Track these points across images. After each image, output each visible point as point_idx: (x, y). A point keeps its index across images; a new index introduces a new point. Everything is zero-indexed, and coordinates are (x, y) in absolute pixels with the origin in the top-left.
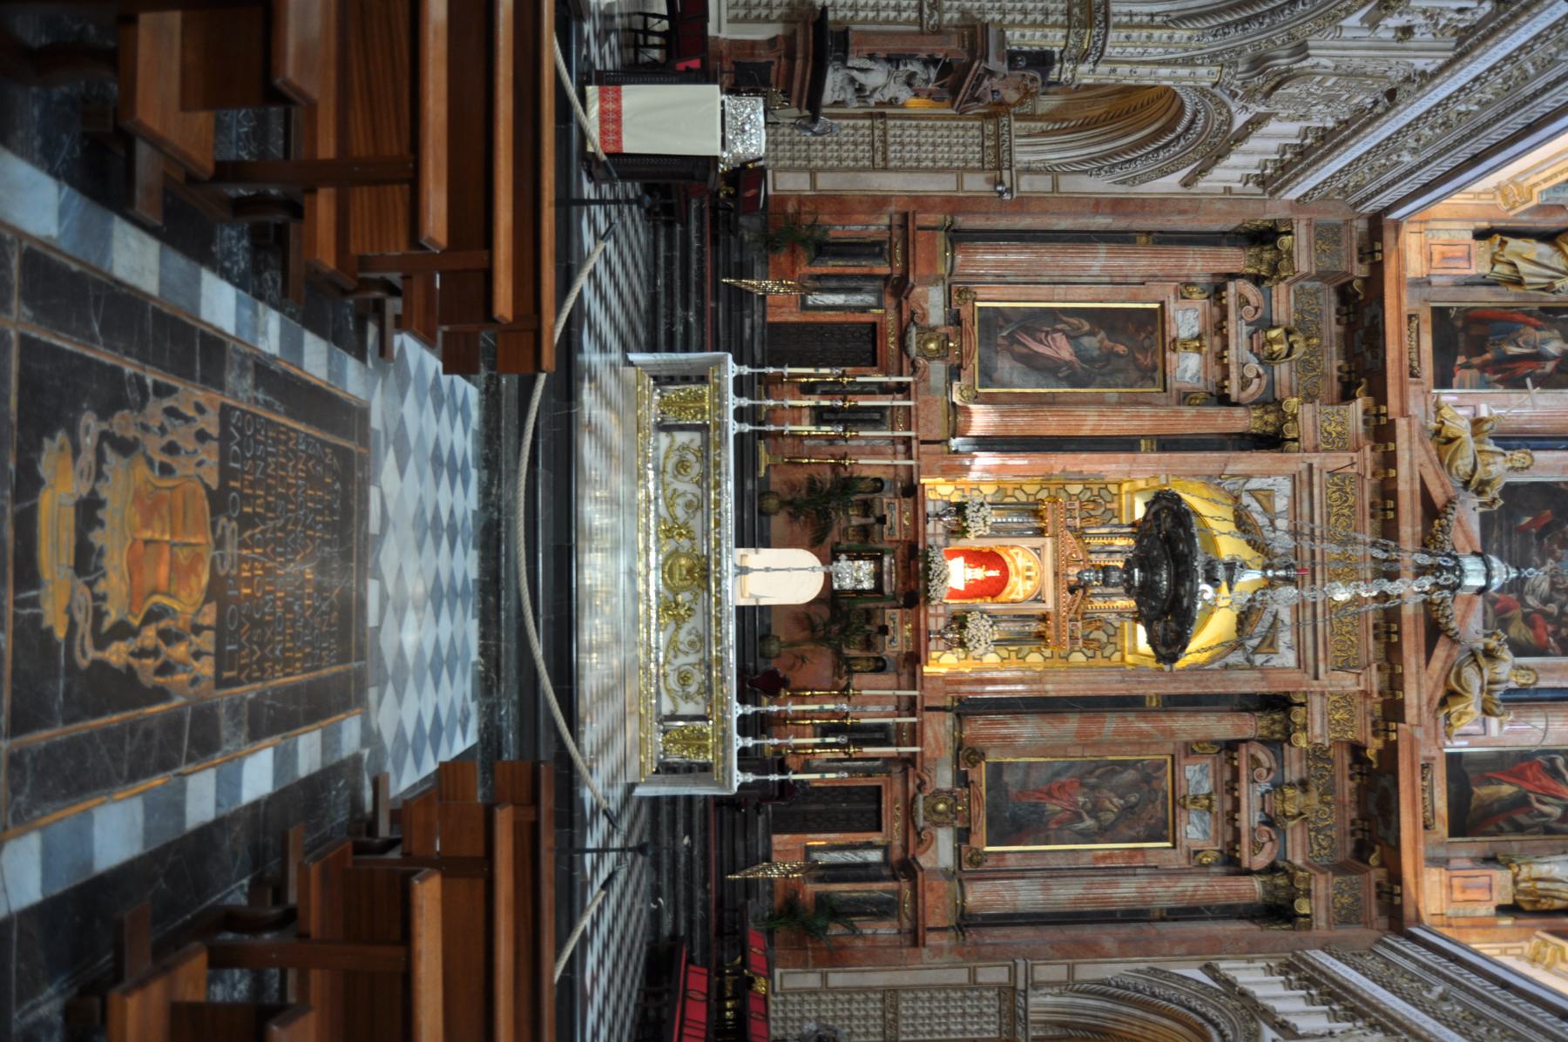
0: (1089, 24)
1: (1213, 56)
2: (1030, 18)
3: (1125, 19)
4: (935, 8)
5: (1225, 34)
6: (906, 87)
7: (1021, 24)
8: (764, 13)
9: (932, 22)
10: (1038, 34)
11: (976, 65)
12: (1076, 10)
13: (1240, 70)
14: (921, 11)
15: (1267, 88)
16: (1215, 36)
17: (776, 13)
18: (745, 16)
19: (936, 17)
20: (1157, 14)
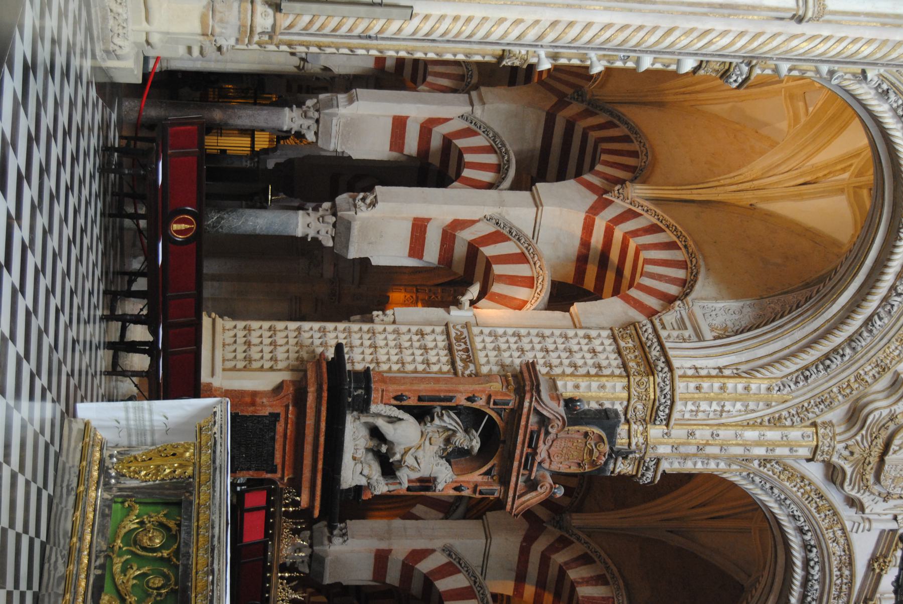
0: (651, 370)
1: (801, 411)
2: (582, 371)
3: (690, 372)
4: (471, 361)
5: (806, 378)
6: (444, 461)
7: (572, 375)
8: (267, 365)
9: (467, 372)
10: (595, 385)
11: (526, 404)
12: (632, 364)
13: (838, 430)
14: (453, 363)
15: (874, 460)
16: (797, 383)
17: (281, 365)
18: (245, 367)
19: (472, 367)
20: (725, 367)
